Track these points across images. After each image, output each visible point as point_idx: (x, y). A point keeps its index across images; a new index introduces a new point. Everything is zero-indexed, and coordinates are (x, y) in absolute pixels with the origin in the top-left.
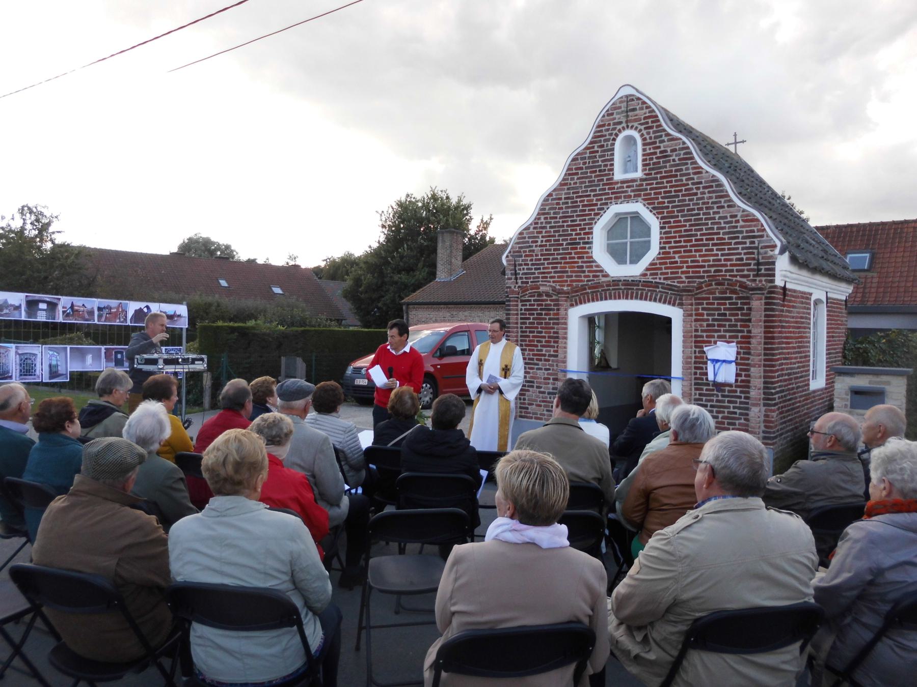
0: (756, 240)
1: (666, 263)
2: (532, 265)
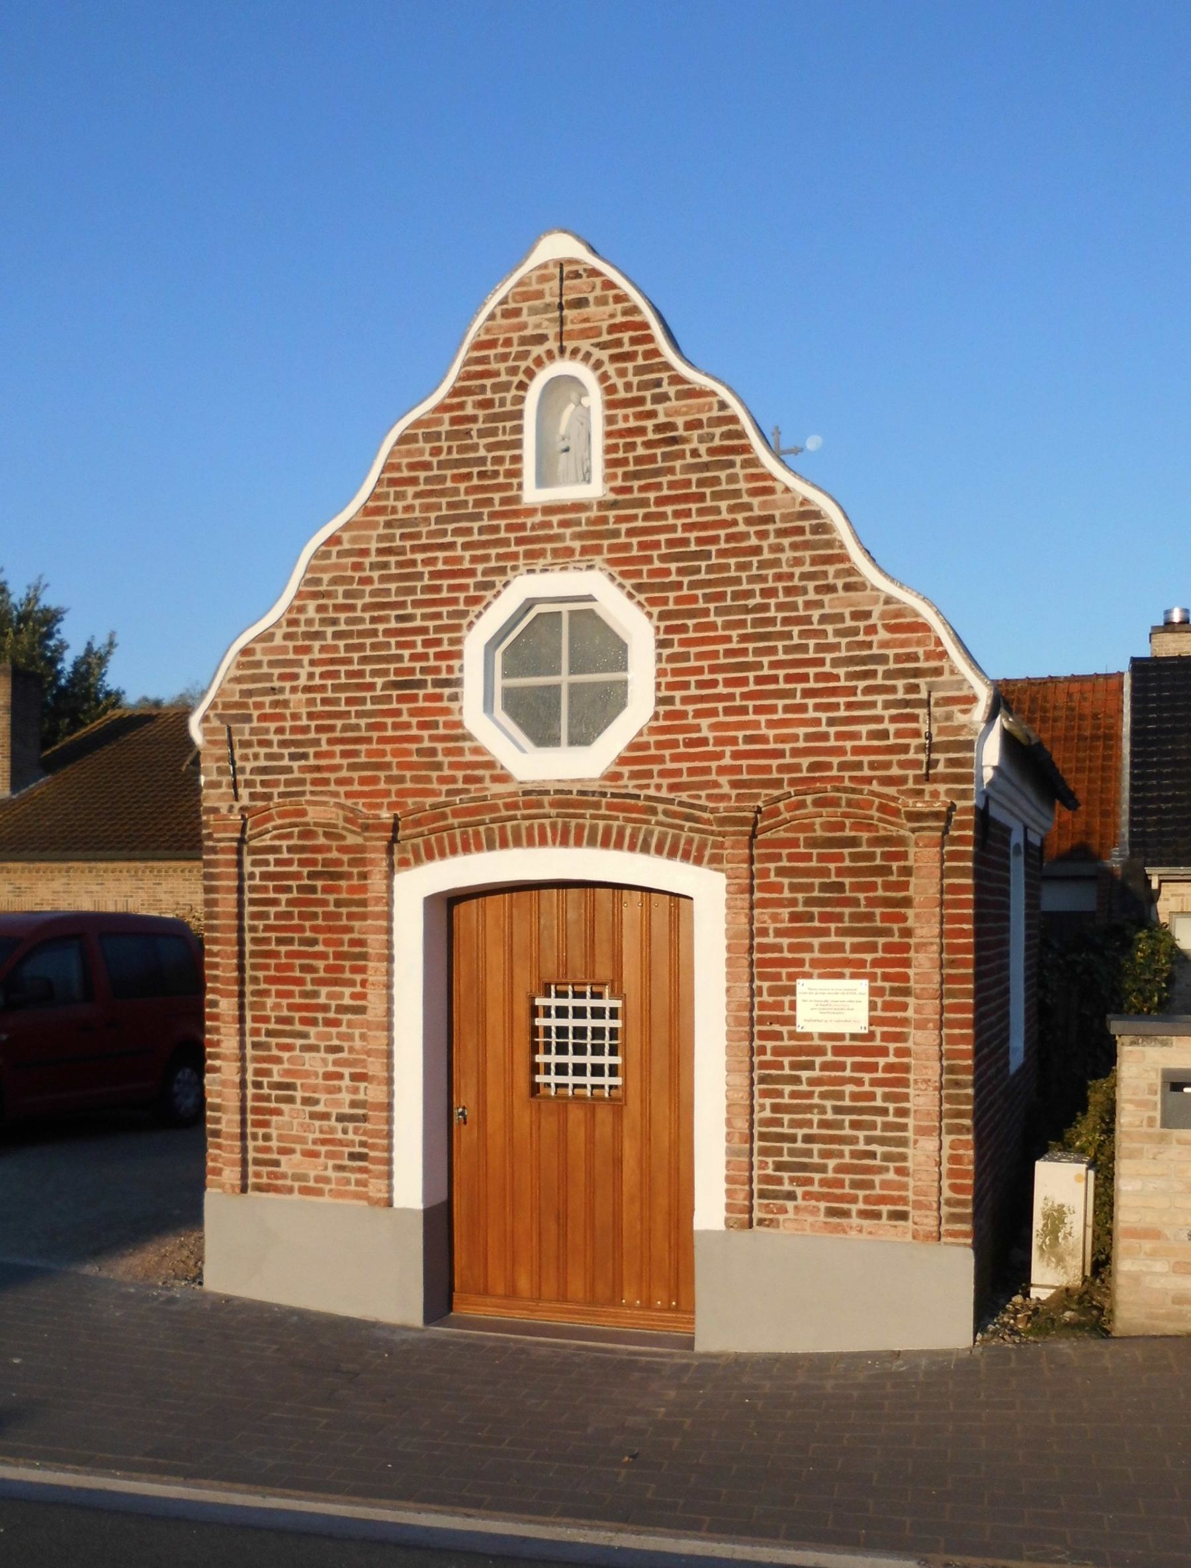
0: (922, 682)
1: (674, 744)
2: (283, 744)
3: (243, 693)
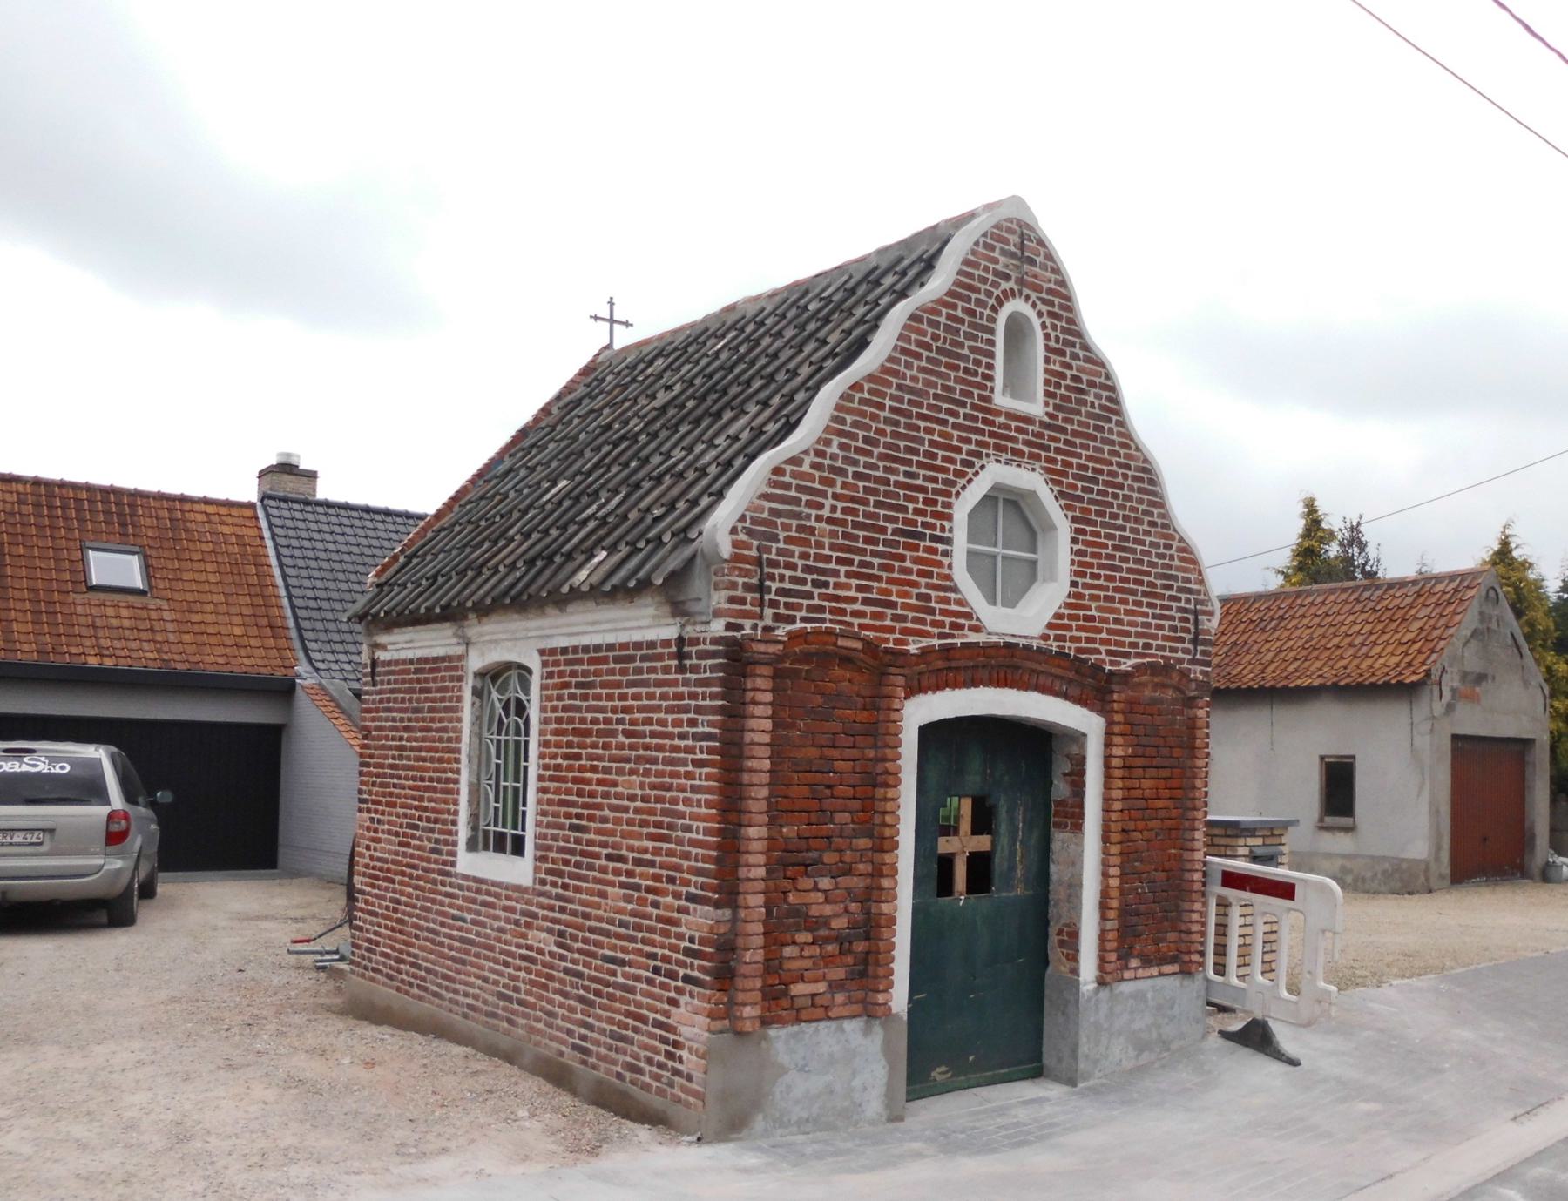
2: (807, 569)
3: (773, 512)
